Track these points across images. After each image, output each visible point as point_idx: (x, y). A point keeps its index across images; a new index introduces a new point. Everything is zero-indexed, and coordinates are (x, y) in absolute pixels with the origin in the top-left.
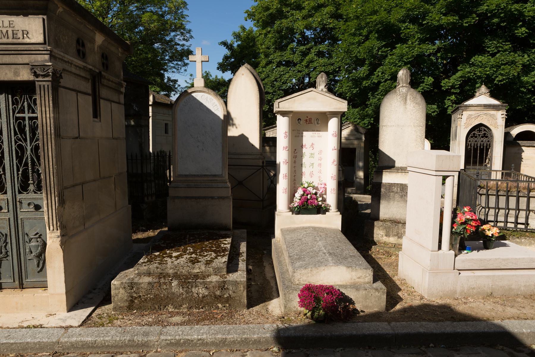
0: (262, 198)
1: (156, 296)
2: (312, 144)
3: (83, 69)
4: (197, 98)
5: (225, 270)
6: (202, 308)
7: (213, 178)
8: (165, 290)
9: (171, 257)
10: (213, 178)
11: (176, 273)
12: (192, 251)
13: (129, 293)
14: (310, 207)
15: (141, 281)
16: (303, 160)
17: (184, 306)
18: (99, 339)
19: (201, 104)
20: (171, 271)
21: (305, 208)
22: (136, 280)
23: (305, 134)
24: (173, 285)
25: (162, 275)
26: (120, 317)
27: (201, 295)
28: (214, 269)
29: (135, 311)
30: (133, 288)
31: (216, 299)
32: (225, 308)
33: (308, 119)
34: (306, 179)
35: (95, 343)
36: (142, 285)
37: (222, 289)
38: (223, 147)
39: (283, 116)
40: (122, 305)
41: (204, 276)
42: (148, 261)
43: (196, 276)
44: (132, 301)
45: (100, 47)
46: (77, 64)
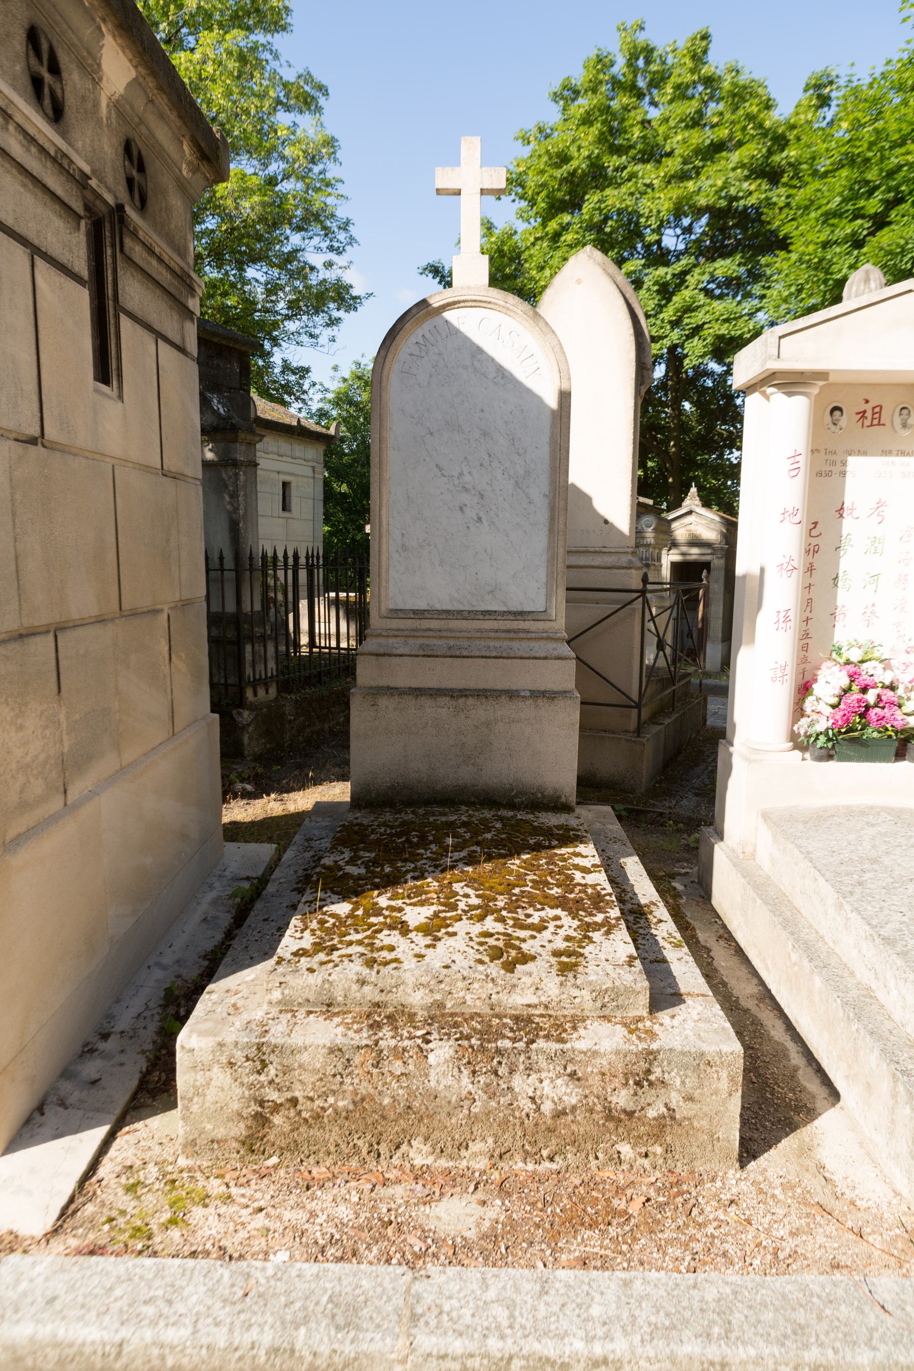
0: (635, 696)
1: (359, 1102)
2: (880, 504)
3: (54, 160)
4: (463, 329)
5: (644, 999)
6: (551, 1159)
7: (515, 625)
8: (398, 1078)
9: (404, 929)
10: (515, 625)
11: (441, 1005)
12: (475, 901)
13: (251, 1086)
14: (871, 733)
15: (297, 1039)
16: (842, 561)
17: (475, 1147)
18: (138, 1338)
19: (477, 351)
20: (419, 994)
21: (854, 740)
22: (277, 1034)
23: (854, 462)
24: (432, 1058)
25: (381, 1016)
26: (215, 1187)
27: (547, 1107)
28: (598, 993)
29: (274, 1160)
30: (264, 1064)
31: (611, 1125)
32: (646, 1163)
33: (868, 407)
34: (848, 633)
35: (119, 1354)
36: (305, 1057)
37: (638, 1084)
38: (552, 508)
39: (789, 394)
40: (220, 1133)
41: (562, 1027)
42: (318, 947)
43: (525, 1024)
44: (261, 1120)
45: (117, 106)
46: (31, 131)
